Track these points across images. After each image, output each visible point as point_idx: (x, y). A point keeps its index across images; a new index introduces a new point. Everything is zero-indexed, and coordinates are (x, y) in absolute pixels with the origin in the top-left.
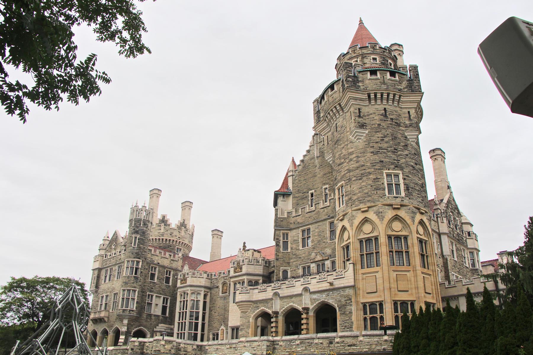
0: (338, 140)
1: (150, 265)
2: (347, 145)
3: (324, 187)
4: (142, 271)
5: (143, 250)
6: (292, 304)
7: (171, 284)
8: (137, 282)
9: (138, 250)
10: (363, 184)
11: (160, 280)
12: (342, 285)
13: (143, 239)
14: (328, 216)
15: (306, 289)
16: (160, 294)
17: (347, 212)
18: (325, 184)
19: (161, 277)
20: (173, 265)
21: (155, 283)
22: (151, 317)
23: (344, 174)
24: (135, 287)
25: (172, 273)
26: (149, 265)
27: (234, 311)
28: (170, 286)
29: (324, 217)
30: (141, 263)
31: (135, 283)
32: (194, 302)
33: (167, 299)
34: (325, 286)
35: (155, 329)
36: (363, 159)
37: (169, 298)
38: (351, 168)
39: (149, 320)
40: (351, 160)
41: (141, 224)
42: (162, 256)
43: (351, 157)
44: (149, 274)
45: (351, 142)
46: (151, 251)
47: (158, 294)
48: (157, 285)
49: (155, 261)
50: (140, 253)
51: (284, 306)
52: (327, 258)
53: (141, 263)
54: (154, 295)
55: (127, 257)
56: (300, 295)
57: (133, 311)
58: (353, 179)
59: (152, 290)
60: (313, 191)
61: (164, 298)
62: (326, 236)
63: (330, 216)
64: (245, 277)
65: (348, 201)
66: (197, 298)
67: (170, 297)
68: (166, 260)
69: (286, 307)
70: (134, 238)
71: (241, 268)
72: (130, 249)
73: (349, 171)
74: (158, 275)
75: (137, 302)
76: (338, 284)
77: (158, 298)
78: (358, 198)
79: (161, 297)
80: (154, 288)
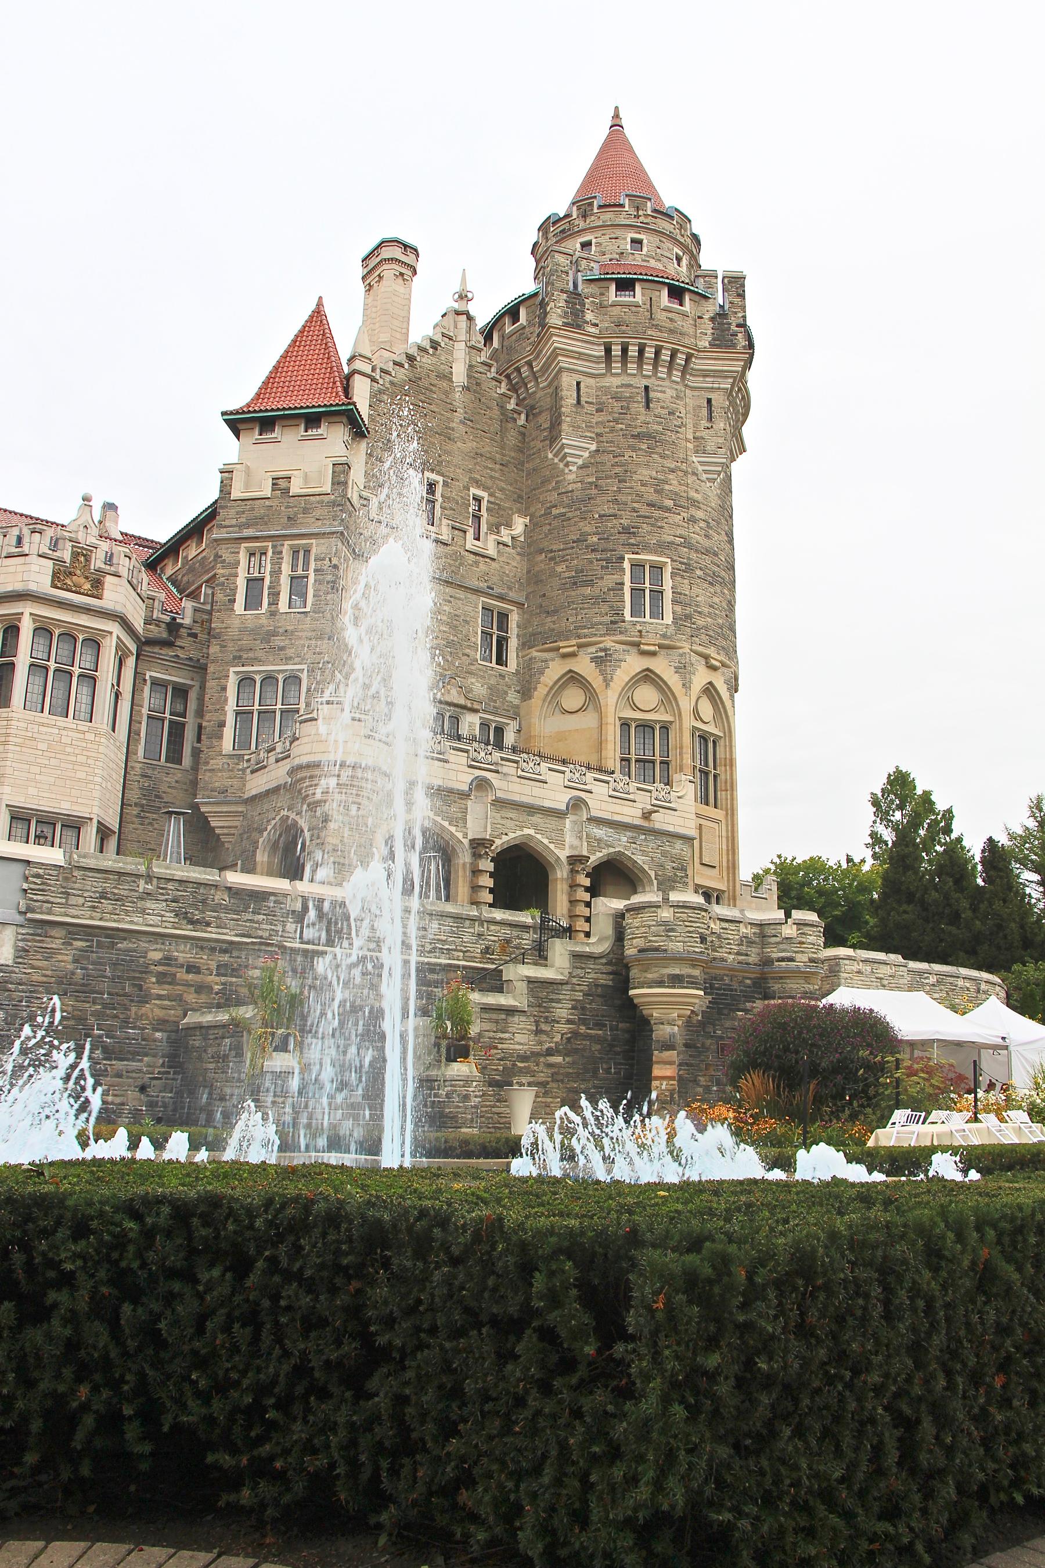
0: (649, 436)
2: (686, 473)
3: (473, 491)
6: (531, 832)
10: (716, 600)
12: (671, 829)
14: (488, 587)
15: (577, 804)
17: (678, 644)
18: (478, 484)
23: (673, 543)
27: (43, 746)
29: (475, 583)
34: (630, 814)
36: (716, 537)
38: (693, 541)
40: (693, 520)
43: (693, 511)
45: (694, 474)
51: (506, 831)
52: (476, 706)
56: (559, 814)
58: (699, 573)
60: (440, 479)
62: (473, 639)
63: (492, 589)
64: (115, 628)
65: (681, 619)
69: (512, 835)
71: (97, 584)
73: (688, 544)
76: (662, 821)
78: (706, 628)
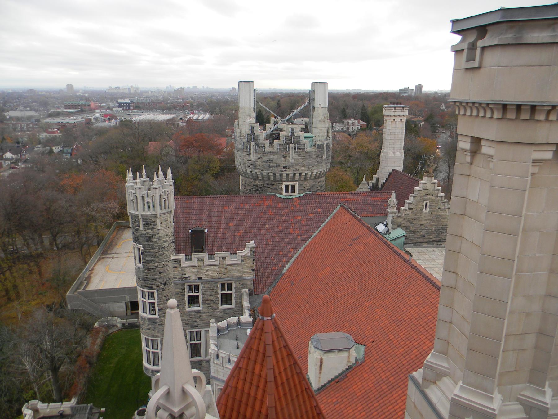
4: (161, 306)
8: (155, 328)
11: (209, 304)
13: (149, 252)
22: (201, 365)
24: (153, 336)
31: (152, 328)
50: (150, 279)
74: (203, 297)
80: (198, 320)
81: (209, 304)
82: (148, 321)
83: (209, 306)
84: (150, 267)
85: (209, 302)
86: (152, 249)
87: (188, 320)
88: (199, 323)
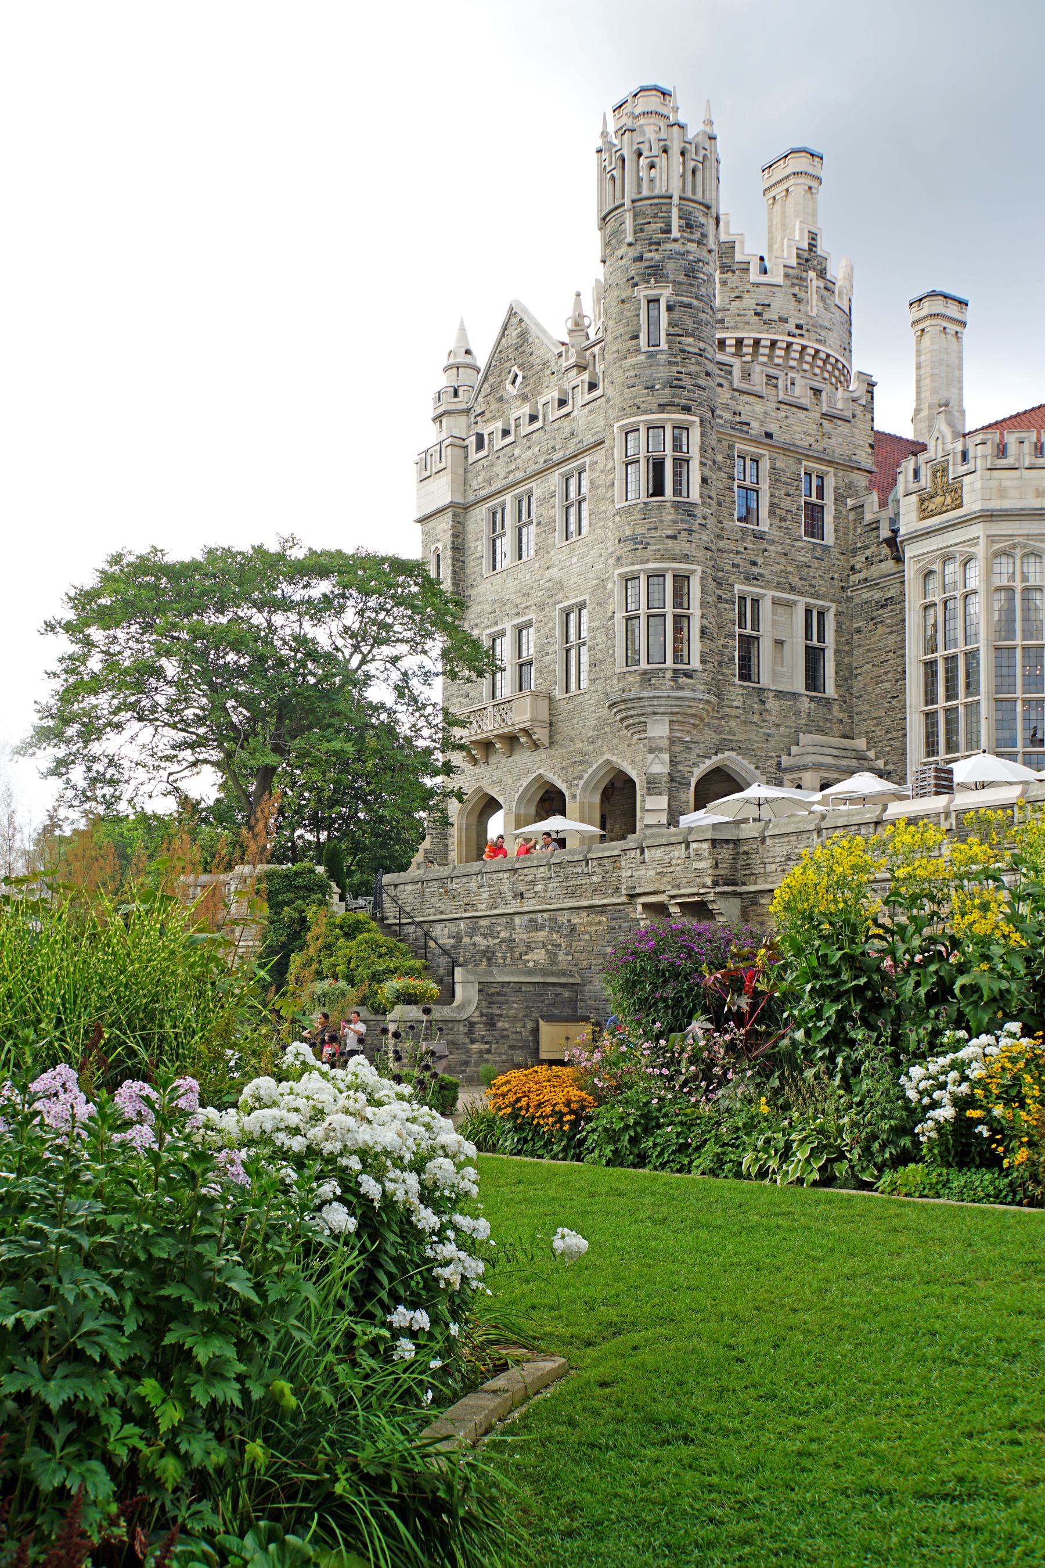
1: (731, 447)
4: (707, 473)
5: (698, 363)
7: (829, 539)
8: (690, 532)
9: (676, 364)
13: (689, 306)
16: (793, 589)
19: (787, 503)
20: (833, 441)
21: (759, 536)
22: (763, 702)
24: (686, 558)
25: (830, 483)
26: (725, 443)
28: (826, 548)
30: (695, 434)
31: (684, 534)
32: (1011, 599)
33: (821, 615)
35: (785, 761)
37: (828, 609)
39: (756, 718)
41: (669, 225)
42: (782, 396)
44: (731, 489)
46: (730, 373)
47: (783, 590)
48: (771, 548)
49: (754, 424)
50: (687, 382)
53: (695, 434)
54: (763, 596)
55: (623, 412)
57: (689, 674)
59: (755, 570)
61: (808, 612)
66: (1025, 578)
67: (833, 605)
68: (802, 414)
70: (644, 305)
72: (634, 367)
75: (704, 633)
77: (781, 610)
79: (790, 605)
80: (760, 560)
81: (783, 519)
82: (672, 511)
83: (783, 524)
84: (688, 349)
85: (783, 512)
86: (697, 299)
87: (738, 552)
88: (761, 571)
